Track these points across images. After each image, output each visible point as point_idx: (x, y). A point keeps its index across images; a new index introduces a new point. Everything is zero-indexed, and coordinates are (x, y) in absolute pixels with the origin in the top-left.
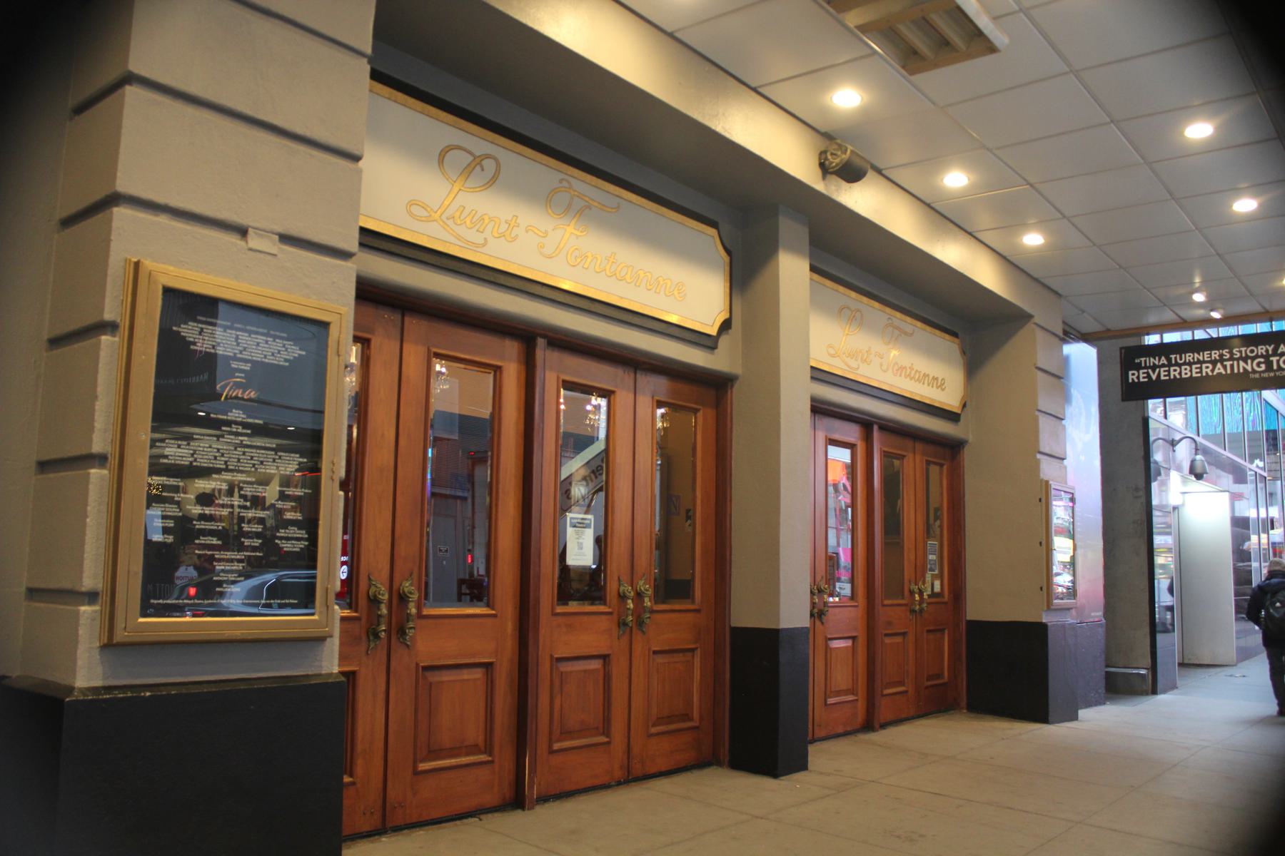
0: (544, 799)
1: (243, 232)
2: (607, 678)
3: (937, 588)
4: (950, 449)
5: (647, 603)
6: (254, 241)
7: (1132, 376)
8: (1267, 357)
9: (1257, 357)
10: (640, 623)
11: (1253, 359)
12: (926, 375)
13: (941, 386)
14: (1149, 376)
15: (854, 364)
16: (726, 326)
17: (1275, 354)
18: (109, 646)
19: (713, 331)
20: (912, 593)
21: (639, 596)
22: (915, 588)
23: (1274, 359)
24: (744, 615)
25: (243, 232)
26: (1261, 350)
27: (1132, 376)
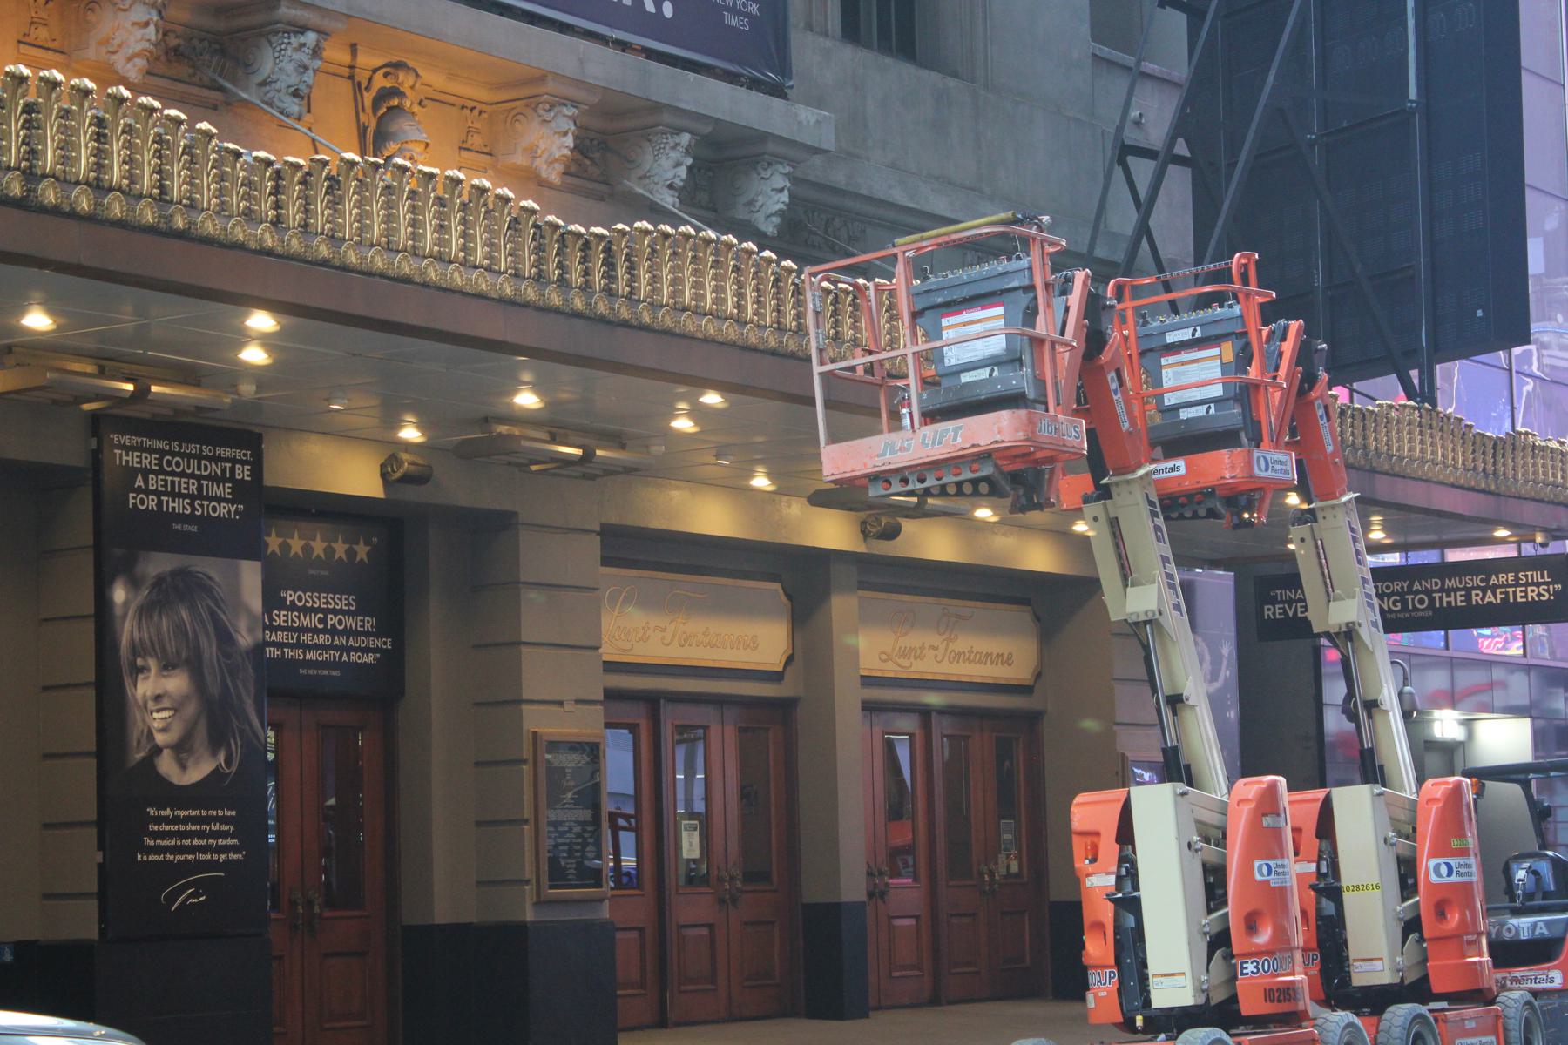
0: (678, 1024)
1: (561, 703)
2: (712, 939)
3: (1015, 867)
4: (1032, 719)
5: (739, 885)
6: (567, 707)
7: (1268, 612)
8: (1402, 594)
9: (1393, 594)
10: (734, 900)
11: (1389, 596)
12: (988, 655)
13: (1007, 661)
14: (1285, 613)
15: (905, 663)
16: (790, 660)
17: (1410, 592)
18: (540, 903)
19: (780, 668)
20: (981, 875)
21: (732, 878)
22: (985, 869)
23: (1409, 597)
24: (813, 893)
25: (561, 703)
26: (1396, 586)
27: (1268, 612)
